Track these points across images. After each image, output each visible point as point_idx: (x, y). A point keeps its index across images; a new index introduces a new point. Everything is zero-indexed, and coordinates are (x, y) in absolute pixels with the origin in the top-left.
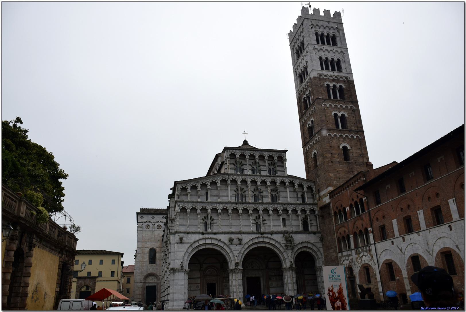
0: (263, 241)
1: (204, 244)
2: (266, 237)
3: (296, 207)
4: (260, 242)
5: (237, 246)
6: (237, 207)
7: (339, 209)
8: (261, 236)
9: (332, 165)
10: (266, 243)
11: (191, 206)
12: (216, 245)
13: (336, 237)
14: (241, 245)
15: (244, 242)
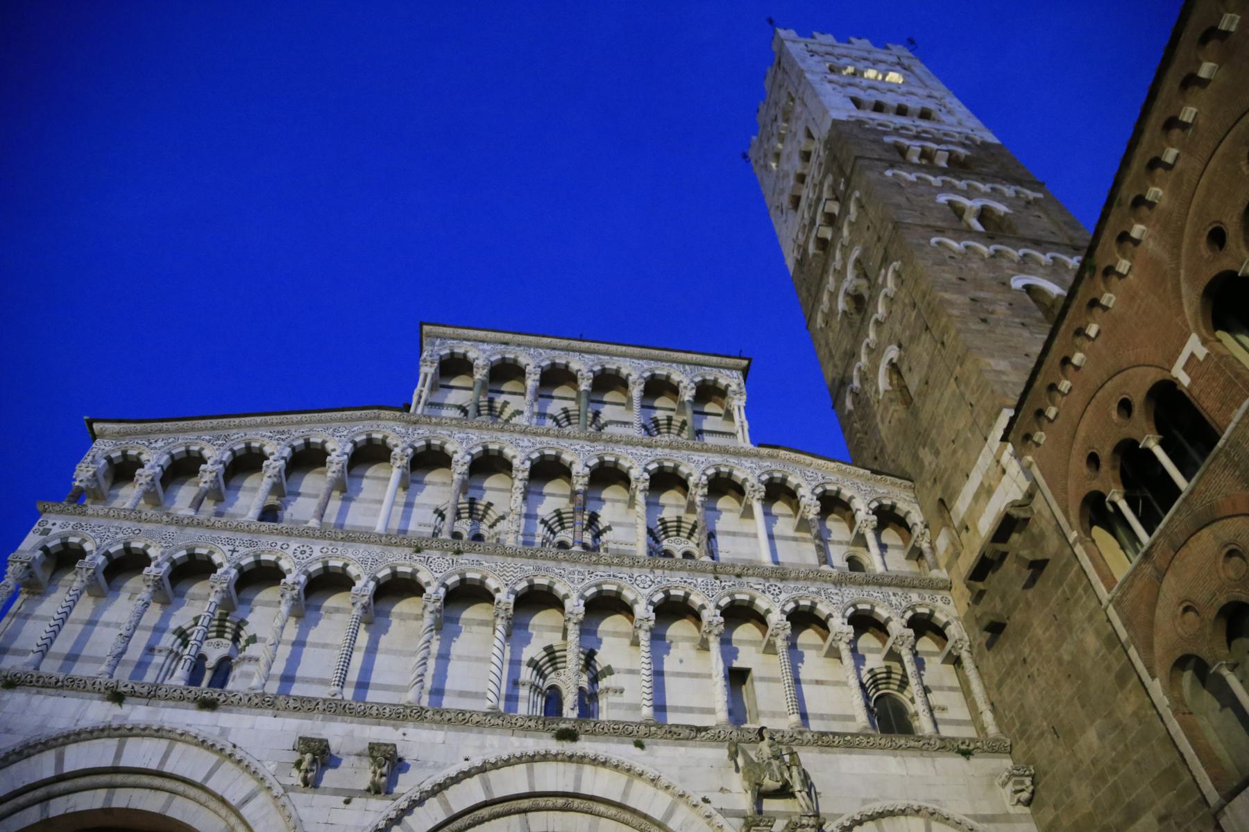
0: (570, 789)
1: (105, 779)
2: (595, 761)
3: (818, 593)
4: (551, 802)
5: (347, 802)
6: (418, 566)
7: (1105, 453)
8: (554, 746)
9: (989, 331)
10: (601, 808)
11: (120, 535)
12: (193, 792)
13: (1153, 677)
14: (388, 802)
15: (407, 785)
